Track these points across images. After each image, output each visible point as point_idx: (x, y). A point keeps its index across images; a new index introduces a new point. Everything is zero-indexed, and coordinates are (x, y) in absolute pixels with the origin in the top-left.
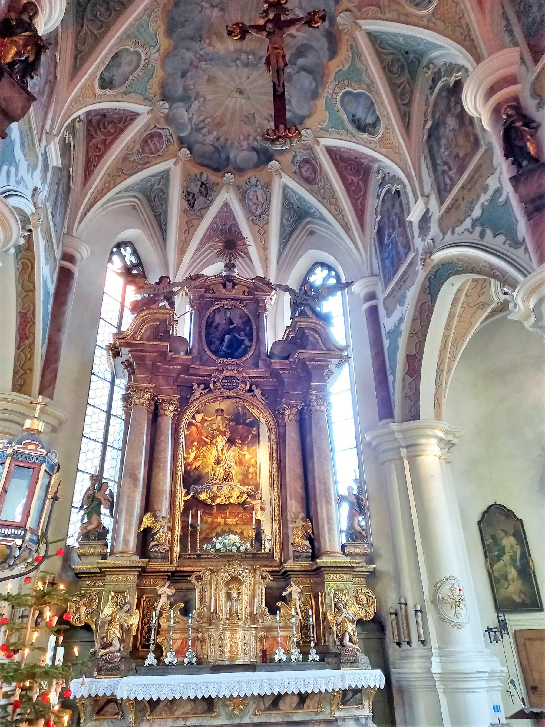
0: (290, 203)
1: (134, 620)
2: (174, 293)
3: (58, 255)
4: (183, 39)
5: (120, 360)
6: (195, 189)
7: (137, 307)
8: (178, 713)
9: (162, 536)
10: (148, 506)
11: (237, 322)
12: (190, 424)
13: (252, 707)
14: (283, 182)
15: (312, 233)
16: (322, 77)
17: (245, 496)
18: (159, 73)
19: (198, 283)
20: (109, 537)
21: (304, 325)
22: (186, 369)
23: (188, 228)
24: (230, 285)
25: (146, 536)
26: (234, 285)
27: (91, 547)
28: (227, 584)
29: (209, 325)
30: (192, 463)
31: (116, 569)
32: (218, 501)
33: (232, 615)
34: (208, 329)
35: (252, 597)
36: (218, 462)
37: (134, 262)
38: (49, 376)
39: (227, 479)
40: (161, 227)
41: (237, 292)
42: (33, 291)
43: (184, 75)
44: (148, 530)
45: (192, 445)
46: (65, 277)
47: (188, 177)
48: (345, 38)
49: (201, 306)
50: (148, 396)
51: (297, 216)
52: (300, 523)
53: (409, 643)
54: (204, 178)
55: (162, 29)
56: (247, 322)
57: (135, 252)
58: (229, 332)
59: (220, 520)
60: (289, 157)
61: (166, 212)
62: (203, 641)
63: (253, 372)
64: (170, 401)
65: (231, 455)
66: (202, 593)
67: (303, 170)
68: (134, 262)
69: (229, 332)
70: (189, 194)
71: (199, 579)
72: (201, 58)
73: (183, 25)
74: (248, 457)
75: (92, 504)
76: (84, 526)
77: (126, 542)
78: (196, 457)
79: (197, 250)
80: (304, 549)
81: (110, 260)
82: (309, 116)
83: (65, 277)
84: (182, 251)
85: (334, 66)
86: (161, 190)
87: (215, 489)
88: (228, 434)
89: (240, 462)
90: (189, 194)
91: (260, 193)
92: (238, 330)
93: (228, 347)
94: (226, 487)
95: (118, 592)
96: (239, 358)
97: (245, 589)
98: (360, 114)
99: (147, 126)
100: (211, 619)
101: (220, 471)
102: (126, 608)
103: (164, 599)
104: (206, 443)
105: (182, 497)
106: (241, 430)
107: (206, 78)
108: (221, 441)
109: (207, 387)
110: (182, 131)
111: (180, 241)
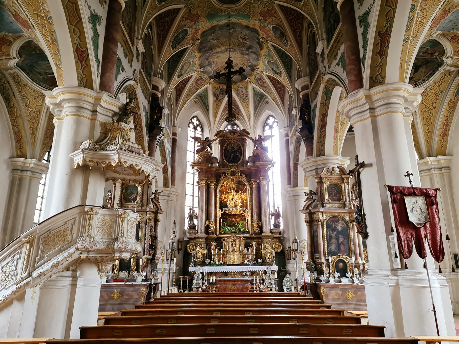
0: (257, 92)
1: (205, 252)
2: (211, 143)
3: (171, 135)
4: (205, 51)
5: (195, 169)
6: (218, 92)
7: (198, 152)
8: (218, 276)
9: (212, 227)
10: (208, 218)
11: (236, 148)
12: (222, 186)
13: (238, 275)
14: (252, 87)
15: (267, 102)
16: (259, 55)
17: (242, 211)
18: (198, 62)
19: (220, 134)
20: (197, 227)
21: (257, 152)
22: (217, 170)
23: (217, 107)
24: (232, 134)
25: (207, 228)
26: (234, 133)
27: (191, 230)
28: (232, 242)
29: (225, 150)
30: (223, 200)
31: (199, 238)
32: (233, 213)
33: (234, 251)
34: (225, 152)
35: (240, 246)
36: (232, 199)
37: (198, 123)
38: (173, 179)
39: (235, 206)
40: (207, 108)
41: (236, 135)
42: (166, 156)
43: (207, 59)
44: (208, 226)
45: (223, 193)
46: (174, 142)
47: (214, 89)
48: (264, 45)
49: (222, 143)
50: (204, 182)
51: (260, 99)
52: (256, 222)
53: (291, 259)
54: (221, 88)
55: (197, 52)
56: (240, 148)
57: (198, 120)
58: (233, 152)
59: (234, 219)
60: (253, 77)
61: (208, 102)
62: (225, 258)
63: (241, 169)
64: (212, 182)
65: (236, 197)
66: (225, 244)
67: (259, 82)
68: (198, 123)
69: (233, 152)
70: (216, 94)
71: (224, 240)
72: (212, 54)
73: (204, 48)
74: (243, 197)
75: (191, 217)
76: (189, 225)
77: (201, 230)
78: (225, 197)
79: (222, 114)
80: (257, 231)
81: (189, 126)
82: (258, 65)
83: (174, 142)
84: (215, 116)
85: (263, 52)
86: (205, 94)
87: (231, 209)
88: (236, 189)
89: (241, 198)
90: (216, 94)
91: (244, 90)
92: (236, 151)
93: (233, 158)
94: (235, 209)
95: (200, 244)
96: (236, 163)
97: (238, 243)
98: (275, 69)
99: (196, 77)
100: (227, 251)
101: (233, 203)
102: (203, 248)
103: (213, 246)
104: (228, 193)
105: (219, 213)
106: (240, 188)
107: (216, 57)
108: (233, 192)
109: (225, 175)
110: (210, 74)
111: (214, 112)
